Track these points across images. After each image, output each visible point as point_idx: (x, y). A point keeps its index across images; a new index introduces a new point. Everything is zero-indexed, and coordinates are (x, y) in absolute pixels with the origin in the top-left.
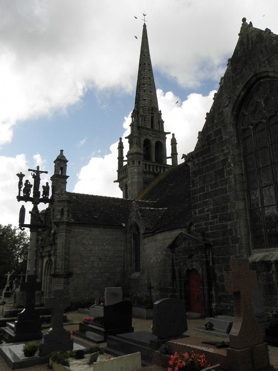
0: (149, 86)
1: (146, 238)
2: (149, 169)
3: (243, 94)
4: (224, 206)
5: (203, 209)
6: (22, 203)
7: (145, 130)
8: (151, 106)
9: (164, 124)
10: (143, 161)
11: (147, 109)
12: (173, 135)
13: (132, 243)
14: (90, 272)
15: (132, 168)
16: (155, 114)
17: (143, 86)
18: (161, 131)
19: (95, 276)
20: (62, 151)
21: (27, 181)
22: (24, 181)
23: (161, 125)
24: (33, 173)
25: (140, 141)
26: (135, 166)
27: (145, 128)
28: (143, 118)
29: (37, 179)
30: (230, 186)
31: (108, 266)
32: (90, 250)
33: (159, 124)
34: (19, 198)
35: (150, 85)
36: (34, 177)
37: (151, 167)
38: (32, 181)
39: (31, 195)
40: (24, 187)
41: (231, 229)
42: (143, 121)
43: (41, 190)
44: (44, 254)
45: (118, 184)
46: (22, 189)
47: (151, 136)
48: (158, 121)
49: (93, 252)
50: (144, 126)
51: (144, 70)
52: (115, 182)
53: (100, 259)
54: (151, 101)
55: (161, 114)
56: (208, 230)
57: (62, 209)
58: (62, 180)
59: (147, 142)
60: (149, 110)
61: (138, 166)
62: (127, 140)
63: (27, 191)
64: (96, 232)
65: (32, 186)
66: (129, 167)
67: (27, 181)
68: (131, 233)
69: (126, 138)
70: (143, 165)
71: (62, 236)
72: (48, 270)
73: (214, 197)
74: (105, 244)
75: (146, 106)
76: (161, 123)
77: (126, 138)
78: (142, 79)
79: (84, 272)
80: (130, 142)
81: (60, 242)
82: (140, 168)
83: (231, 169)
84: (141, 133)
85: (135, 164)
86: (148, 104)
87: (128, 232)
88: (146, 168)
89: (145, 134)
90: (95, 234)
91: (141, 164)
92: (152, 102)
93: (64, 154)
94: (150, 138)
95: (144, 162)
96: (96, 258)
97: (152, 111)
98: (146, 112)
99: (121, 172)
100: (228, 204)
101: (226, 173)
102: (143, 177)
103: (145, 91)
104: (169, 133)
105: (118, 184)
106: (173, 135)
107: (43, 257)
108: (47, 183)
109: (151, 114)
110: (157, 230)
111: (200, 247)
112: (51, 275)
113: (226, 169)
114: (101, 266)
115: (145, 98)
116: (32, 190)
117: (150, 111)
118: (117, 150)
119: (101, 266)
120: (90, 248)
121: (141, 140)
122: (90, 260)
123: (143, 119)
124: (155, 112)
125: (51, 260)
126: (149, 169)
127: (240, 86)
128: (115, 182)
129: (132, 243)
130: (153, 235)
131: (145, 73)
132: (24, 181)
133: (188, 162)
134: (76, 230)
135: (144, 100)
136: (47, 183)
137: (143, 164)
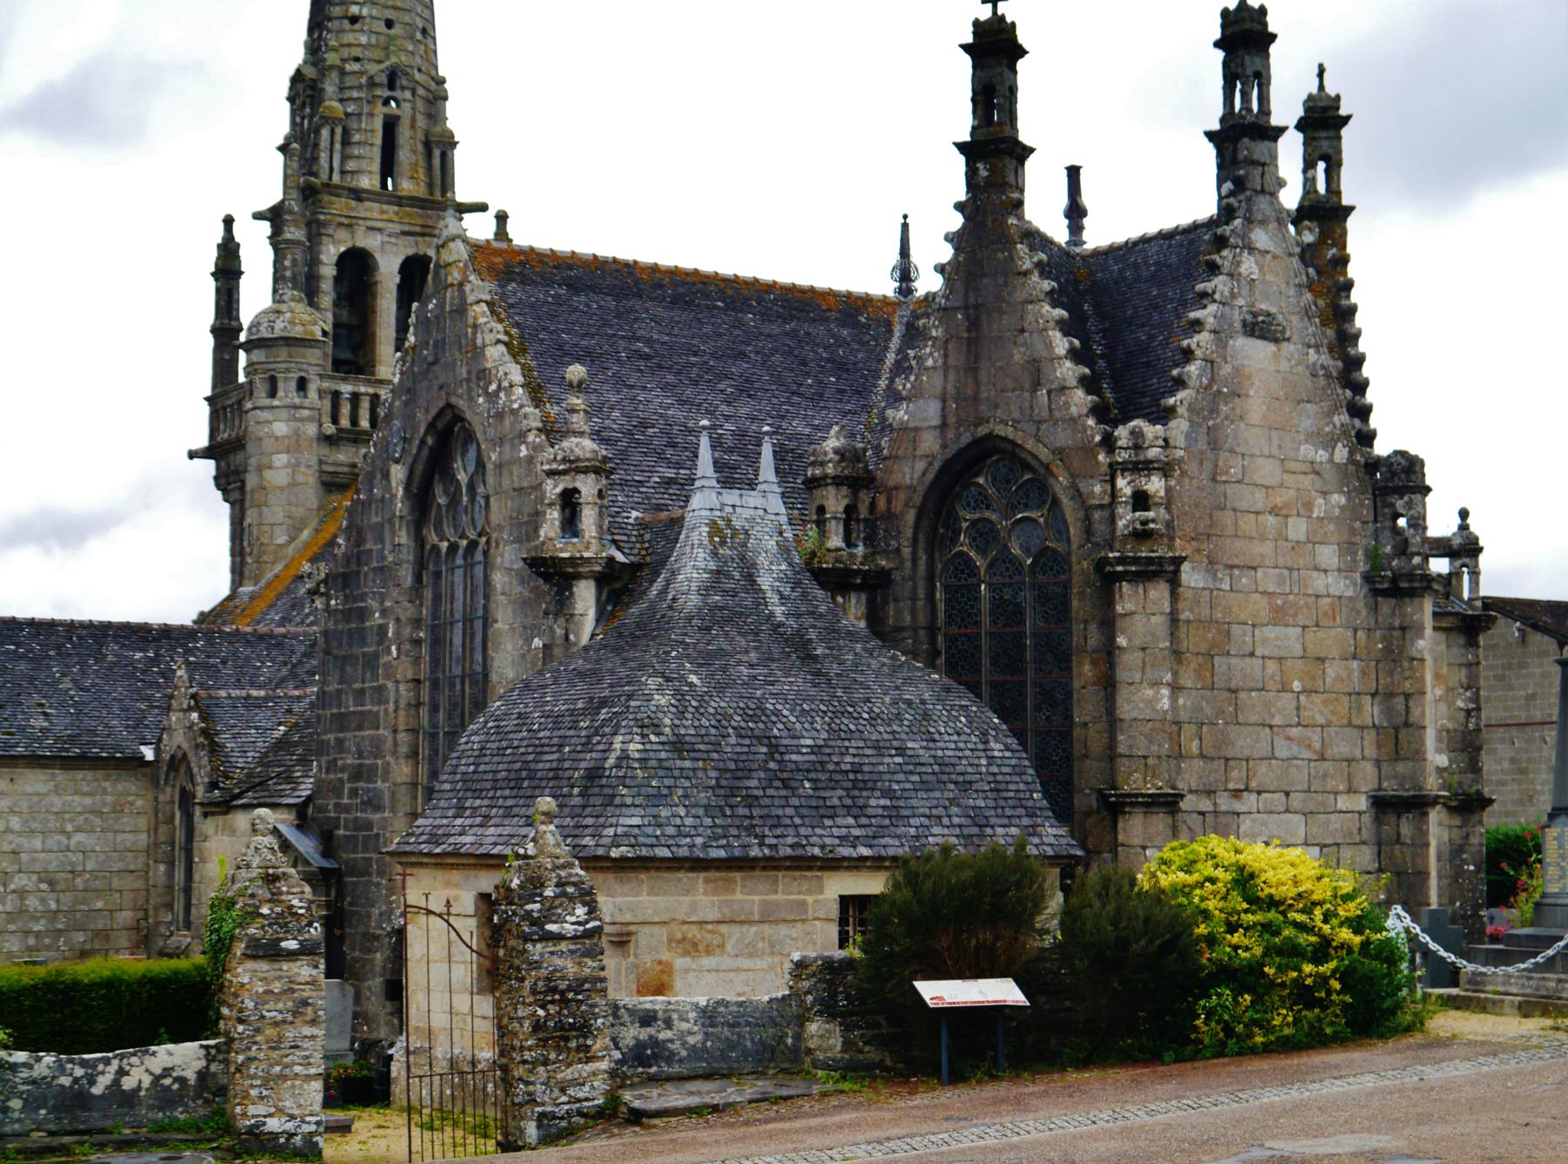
1: (210, 819)
2: (354, 421)
5: (335, 759)
8: (388, 57)
9: (459, 156)
10: (321, 376)
11: (364, 80)
12: (502, 218)
13: (177, 822)
14: (12, 927)
16: (407, 106)
18: (438, 196)
19: (31, 941)
23: (437, 162)
25: (313, 262)
26: (276, 403)
27: (343, 188)
28: (339, 130)
30: (386, 710)
31: (83, 907)
32: (14, 852)
33: (429, 155)
37: (365, 405)
41: (378, 834)
42: (338, 146)
45: (209, 466)
47: (379, 230)
48: (420, 135)
49: (24, 857)
50: (343, 172)
52: (192, 455)
53: (51, 883)
54: (389, 24)
55: (445, 98)
56: (338, 828)
60: (372, 84)
61: (296, 407)
62: (265, 227)
64: (35, 782)
68: (174, 786)
69: (258, 216)
70: (320, 397)
74: (69, 828)
76: (437, 153)
77: (258, 216)
80: (275, 240)
82: (306, 413)
84: (322, 217)
85: (280, 393)
86: (369, 46)
87: (162, 782)
88: (335, 420)
89: (346, 221)
90: (29, 789)
91: (313, 394)
92: (396, 37)
94: (370, 242)
95: (326, 385)
96: (34, 878)
99: (224, 409)
102: (321, 462)
104: (482, 208)
105: (209, 466)
106: (502, 218)
114: (53, 906)
117: (378, 92)
118: (211, 285)
119: (53, 906)
120: (10, 843)
121: (324, 258)
122: (12, 887)
123: (338, 137)
126: (354, 421)
127: (423, 419)
128: (192, 455)
129: (177, 822)
130: (226, 813)
135: (354, 20)
137: (321, 392)
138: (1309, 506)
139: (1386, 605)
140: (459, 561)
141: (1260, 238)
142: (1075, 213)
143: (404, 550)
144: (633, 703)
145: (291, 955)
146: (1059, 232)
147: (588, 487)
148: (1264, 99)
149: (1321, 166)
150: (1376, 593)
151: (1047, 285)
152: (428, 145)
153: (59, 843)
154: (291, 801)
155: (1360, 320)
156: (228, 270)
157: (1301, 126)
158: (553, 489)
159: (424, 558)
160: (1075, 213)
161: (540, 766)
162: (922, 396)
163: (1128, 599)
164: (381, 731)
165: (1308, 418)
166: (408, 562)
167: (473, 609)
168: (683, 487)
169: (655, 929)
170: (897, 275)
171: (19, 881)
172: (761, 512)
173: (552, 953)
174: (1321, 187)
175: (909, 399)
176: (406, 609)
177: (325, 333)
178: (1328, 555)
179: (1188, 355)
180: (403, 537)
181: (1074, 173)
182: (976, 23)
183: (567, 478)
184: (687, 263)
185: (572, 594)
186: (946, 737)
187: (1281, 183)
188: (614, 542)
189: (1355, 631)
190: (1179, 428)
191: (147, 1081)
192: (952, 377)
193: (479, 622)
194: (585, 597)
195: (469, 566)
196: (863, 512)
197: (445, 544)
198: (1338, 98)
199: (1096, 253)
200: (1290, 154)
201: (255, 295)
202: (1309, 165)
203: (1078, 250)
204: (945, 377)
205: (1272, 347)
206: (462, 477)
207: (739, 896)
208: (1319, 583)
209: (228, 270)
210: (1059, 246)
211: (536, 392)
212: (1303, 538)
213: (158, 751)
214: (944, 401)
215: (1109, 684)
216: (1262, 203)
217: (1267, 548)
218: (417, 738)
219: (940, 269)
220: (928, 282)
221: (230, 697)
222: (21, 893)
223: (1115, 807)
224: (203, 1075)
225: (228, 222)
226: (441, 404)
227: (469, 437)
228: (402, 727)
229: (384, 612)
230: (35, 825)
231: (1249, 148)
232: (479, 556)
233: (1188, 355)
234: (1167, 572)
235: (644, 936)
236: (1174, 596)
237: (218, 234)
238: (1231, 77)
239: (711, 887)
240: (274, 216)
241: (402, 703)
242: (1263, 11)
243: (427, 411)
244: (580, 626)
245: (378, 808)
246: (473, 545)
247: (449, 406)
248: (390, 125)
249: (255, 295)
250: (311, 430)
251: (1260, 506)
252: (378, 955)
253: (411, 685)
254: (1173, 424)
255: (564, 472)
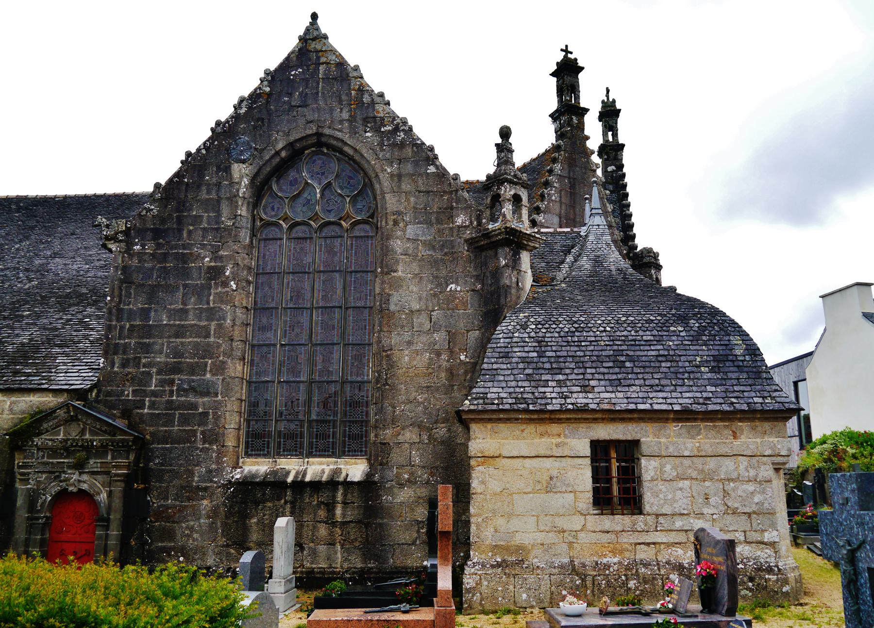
4: (196, 362)
30: (220, 326)
73: (173, 340)
83: (227, 292)
100: (208, 362)
101: (214, 297)
111: (118, 443)
113: (217, 289)
133: (110, 240)
143: (244, 220)
162: (550, 213)
164: (212, 339)
166: (247, 228)
175: (545, 212)
176: (244, 259)
180: (243, 211)
185: (520, 257)
192: (564, 207)
204: (561, 207)
214: (560, 218)
218: (245, 347)
228: (236, 338)
229: (216, 258)
241: (238, 322)
243: (288, 134)
247: (318, 134)
252: (205, 502)
253: (244, 310)
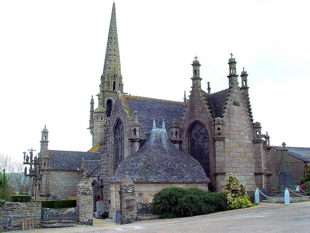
0: (114, 57)
3: (116, 123)
6: (26, 165)
7: (107, 93)
9: (124, 86)
15: (97, 123)
17: (109, 56)
19: (62, 196)
20: (45, 126)
21: (27, 155)
22: (26, 156)
24: (30, 151)
28: (107, 83)
29: (31, 154)
34: (24, 163)
35: (115, 55)
36: (30, 153)
38: (29, 156)
39: (29, 162)
40: (26, 158)
42: (107, 85)
43: (33, 159)
44: (37, 184)
46: (25, 159)
48: (119, 84)
51: (111, 43)
53: (65, 188)
54: (114, 68)
57: (45, 163)
58: (45, 144)
59: (109, 102)
60: (112, 77)
63: (27, 160)
64: (63, 173)
65: (29, 157)
66: (95, 121)
67: (27, 155)
69: (96, 95)
71: (45, 177)
72: (39, 192)
75: (110, 73)
76: (121, 86)
77: (96, 95)
78: (109, 50)
79: (56, 194)
80: (99, 99)
81: (44, 179)
88: (106, 123)
93: (47, 128)
97: (114, 77)
98: (110, 78)
103: (110, 61)
107: (36, 185)
108: (36, 156)
109: (114, 79)
110: (90, 175)
112: (40, 195)
115: (110, 67)
116: (30, 159)
123: (107, 84)
124: (117, 78)
125: (40, 187)
131: (111, 45)
132: (26, 156)
134: (53, 173)
135: (110, 68)
136: (36, 156)
138: (244, 130)
139: (256, 144)
140: (120, 141)
141: (236, 91)
142: (209, 89)
144: (143, 159)
145: (88, 195)
146: (207, 91)
147: (137, 128)
148: (235, 71)
149: (244, 82)
150: (255, 143)
151: (204, 98)
152: (120, 85)
153: (66, 182)
154: (97, 176)
155: (251, 104)
156: (92, 103)
157: (241, 76)
158: (132, 129)
159: (116, 140)
160: (209, 89)
161: (130, 169)
163: (217, 143)
165: (243, 117)
167: (122, 148)
168: (151, 128)
169: (146, 193)
170: (184, 99)
171: (61, 187)
172: (163, 131)
173: (128, 195)
174: (244, 85)
177: (105, 111)
178: (247, 137)
179: (225, 108)
181: (208, 83)
182: (193, 61)
183: (134, 127)
184: (153, 97)
186: (190, 164)
187: (238, 83)
188: (141, 136)
189: (251, 148)
190: (224, 119)
191: (67, 213)
193: (123, 149)
194: (137, 145)
195: (121, 142)
196: (178, 132)
197: (118, 138)
198: (246, 72)
199: (212, 94)
200: (239, 79)
201: (96, 106)
202: (242, 82)
203: (209, 94)
205: (238, 107)
206: (121, 128)
207: (159, 188)
208: (245, 141)
209: (92, 103)
210: (207, 94)
211: (131, 114)
212: (243, 135)
213: (80, 169)
215: (214, 156)
216: (235, 86)
217: (237, 136)
219: (189, 96)
220: (188, 98)
221: (90, 161)
222: (61, 189)
223: (216, 175)
224: (75, 212)
225: (92, 96)
226: (117, 118)
227: (121, 122)
230: (63, 180)
231: (234, 78)
232: (123, 139)
233: (225, 108)
234: (223, 139)
235: (144, 194)
236: (224, 144)
237: (91, 98)
238: (230, 69)
239: (154, 186)
240: (98, 95)
242: (235, 59)
244: (136, 149)
245: (109, 177)
246: (122, 138)
248: (114, 83)
249: (96, 106)
250: (103, 124)
251: (236, 130)
254: (223, 118)
255: (134, 126)
